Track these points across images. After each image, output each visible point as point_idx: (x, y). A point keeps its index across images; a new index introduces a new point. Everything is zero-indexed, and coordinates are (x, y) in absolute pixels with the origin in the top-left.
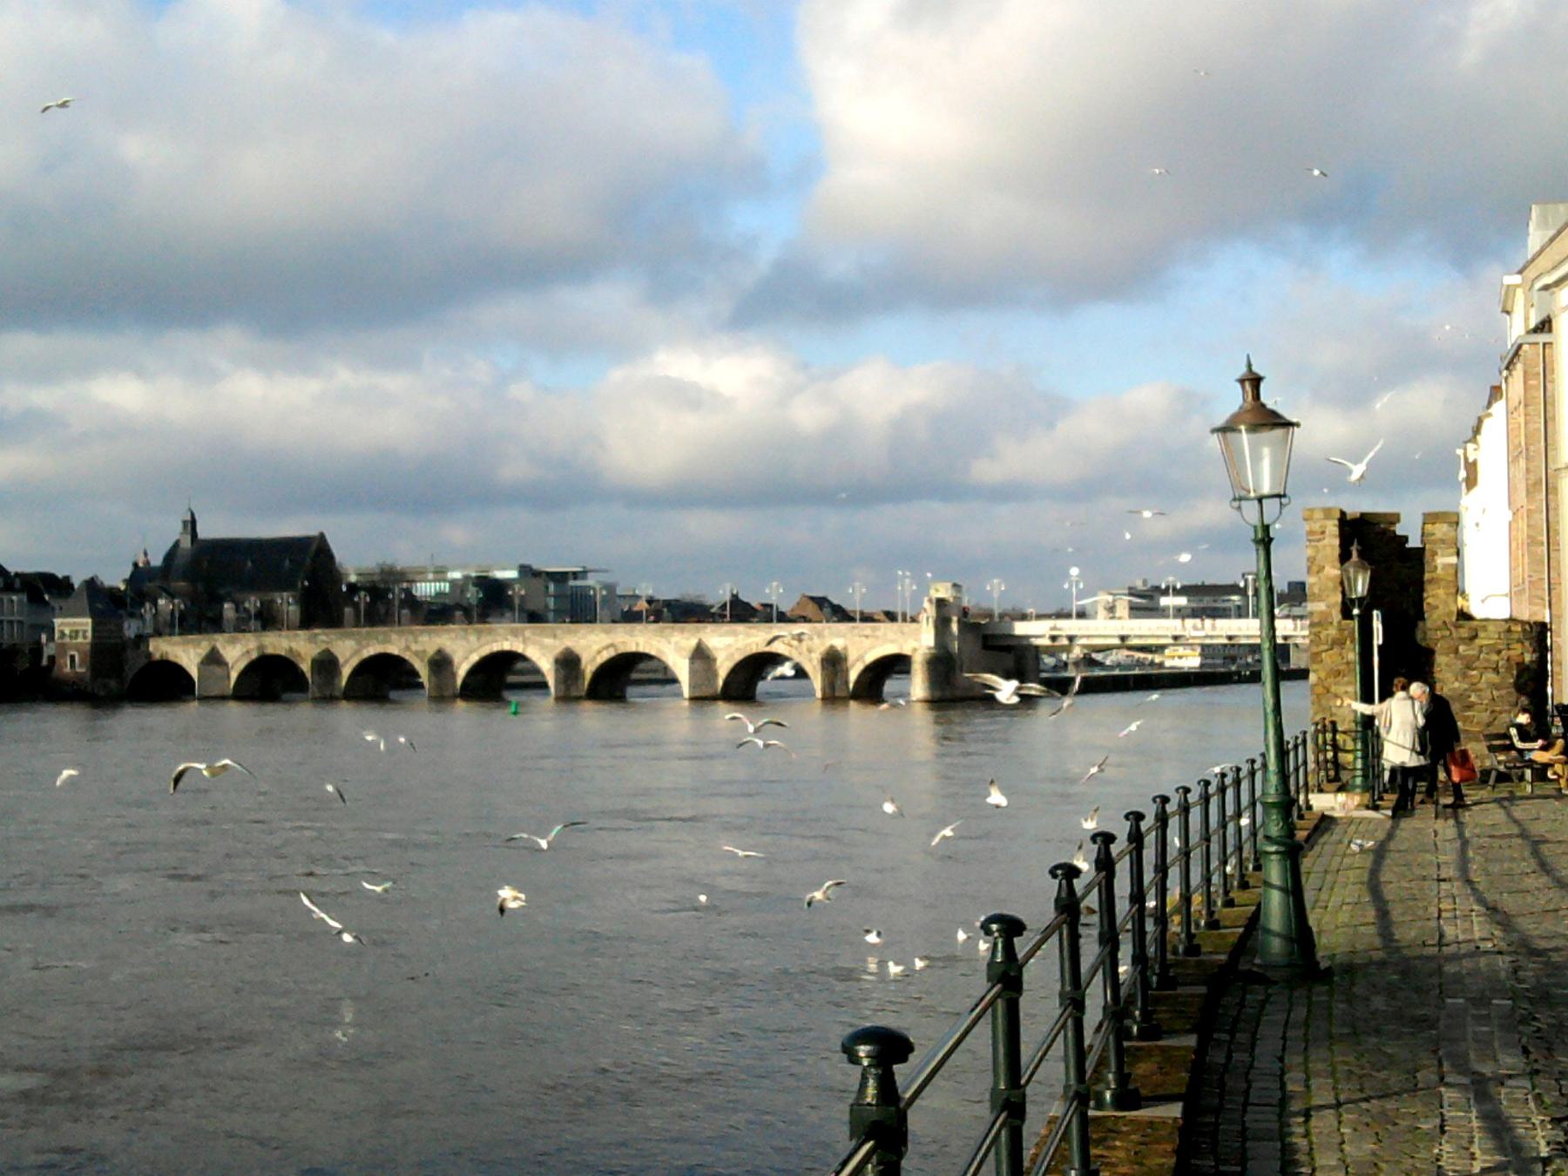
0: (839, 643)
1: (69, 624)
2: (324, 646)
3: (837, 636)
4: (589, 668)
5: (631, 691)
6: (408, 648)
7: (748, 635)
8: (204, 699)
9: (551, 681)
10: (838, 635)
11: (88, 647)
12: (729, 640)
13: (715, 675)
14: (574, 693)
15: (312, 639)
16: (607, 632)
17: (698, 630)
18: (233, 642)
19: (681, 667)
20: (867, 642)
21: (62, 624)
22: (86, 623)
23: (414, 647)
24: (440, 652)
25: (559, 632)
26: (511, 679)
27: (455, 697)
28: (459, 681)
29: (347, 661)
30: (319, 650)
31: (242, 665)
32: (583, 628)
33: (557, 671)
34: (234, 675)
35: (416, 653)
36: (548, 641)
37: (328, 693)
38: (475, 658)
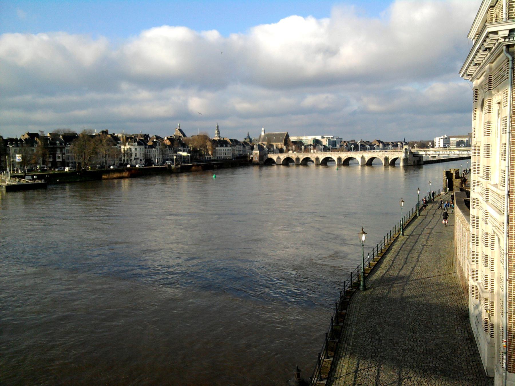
0: (387, 156)
4: (343, 160)
10: (387, 154)
12: (368, 155)
14: (340, 164)
16: (346, 154)
18: (282, 155)
19: (359, 160)
20: (392, 156)
22: (258, 152)
24: (317, 157)
27: (320, 164)
28: (320, 162)
31: (283, 159)
32: (342, 153)
34: (282, 161)
36: (336, 155)
38: (323, 158)
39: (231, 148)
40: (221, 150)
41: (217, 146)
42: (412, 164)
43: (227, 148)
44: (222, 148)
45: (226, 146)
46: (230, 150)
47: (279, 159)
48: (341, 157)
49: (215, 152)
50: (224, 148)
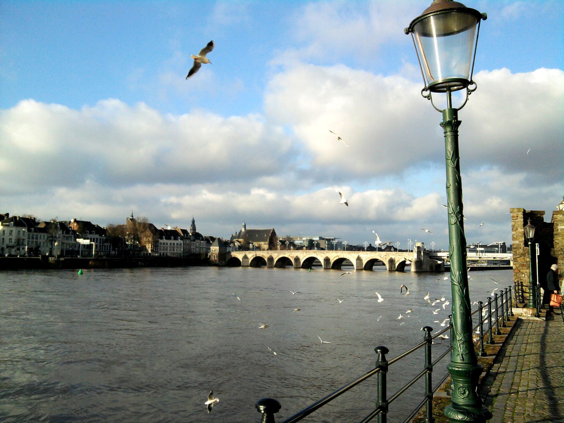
0: (393, 257)
1: (213, 248)
2: (270, 255)
3: (393, 255)
4: (332, 261)
5: (342, 267)
6: (289, 256)
7: (370, 254)
8: (243, 266)
9: (323, 265)
10: (393, 255)
11: (218, 254)
12: (366, 255)
13: (362, 264)
14: (328, 267)
15: (268, 253)
16: (336, 253)
17: (358, 253)
18: (250, 253)
19: (354, 262)
21: (212, 248)
22: (217, 248)
23: (291, 255)
24: (297, 257)
25: (325, 252)
26: (314, 264)
27: (300, 268)
28: (301, 264)
29: (275, 258)
30: (269, 256)
31: (252, 259)
32: (331, 252)
33: (324, 262)
34: (250, 261)
35: (291, 257)
36: (322, 255)
37: (271, 266)
38: (305, 258)
39: (182, 242)
40: (167, 244)
41: (162, 238)
42: (428, 269)
43: (176, 242)
44: (169, 242)
45: (176, 239)
46: (181, 244)
47: (246, 259)
48: (329, 257)
49: (158, 246)
50: (172, 241)
